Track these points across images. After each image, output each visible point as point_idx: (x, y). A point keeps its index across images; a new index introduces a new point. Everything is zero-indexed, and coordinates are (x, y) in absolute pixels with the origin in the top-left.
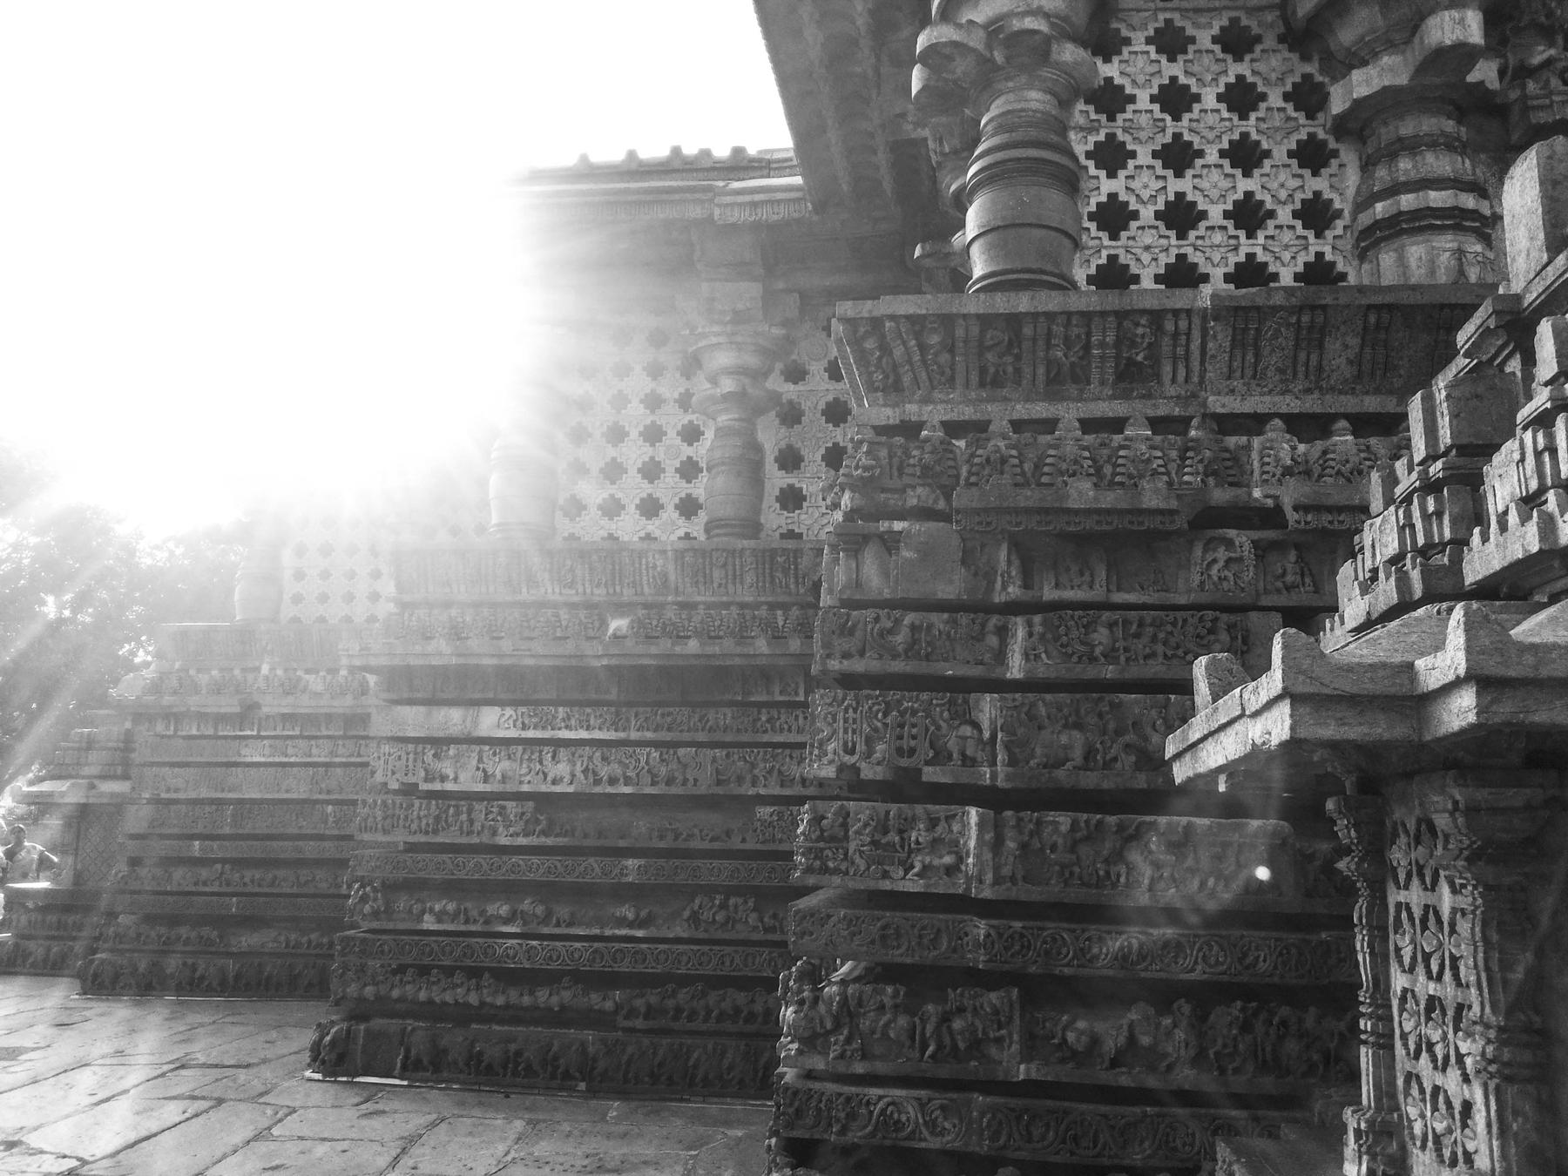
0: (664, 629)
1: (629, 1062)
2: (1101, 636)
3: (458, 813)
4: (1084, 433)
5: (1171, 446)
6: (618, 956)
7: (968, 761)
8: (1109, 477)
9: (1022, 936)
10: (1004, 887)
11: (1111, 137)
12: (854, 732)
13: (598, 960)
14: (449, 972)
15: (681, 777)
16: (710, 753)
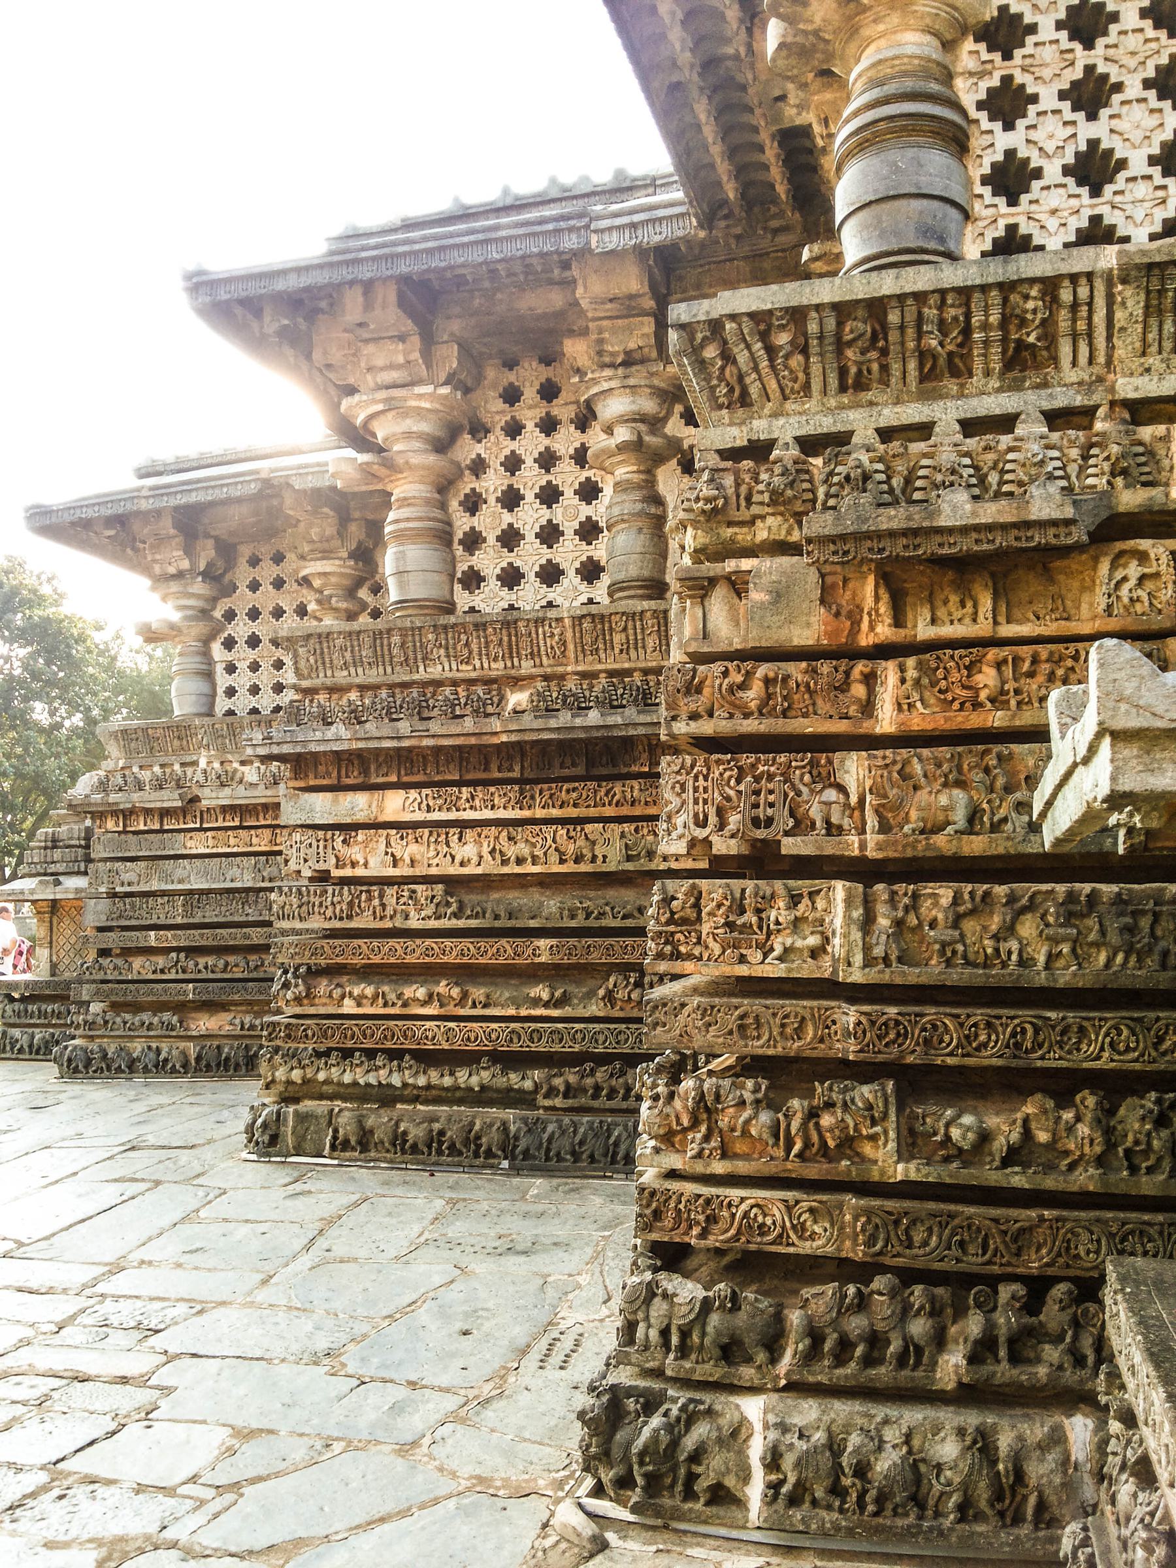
0: (564, 702)
1: (550, 1140)
2: (987, 678)
3: (370, 899)
4: (965, 437)
5: (1072, 443)
6: (535, 1036)
7: (832, 829)
8: (995, 487)
9: (897, 1023)
10: (876, 969)
11: (1007, 80)
12: (705, 802)
14: (371, 1054)
15: (589, 855)
16: (616, 828)
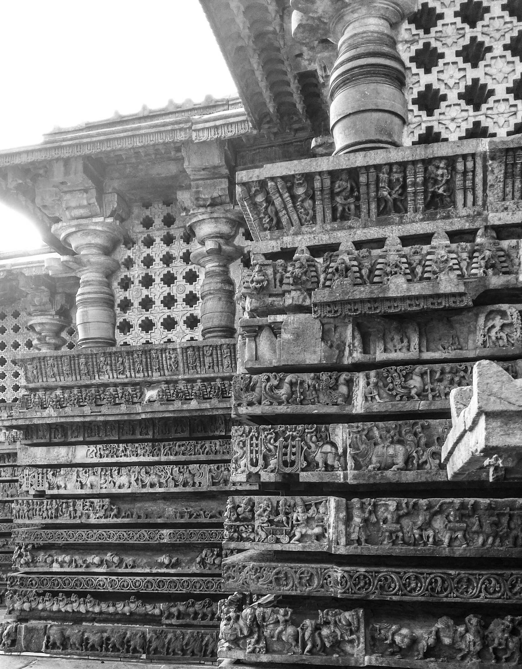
0: (177, 395)
1: (169, 643)
2: (416, 382)
3: (67, 507)
6: (161, 584)
7: (328, 468)
9: (365, 577)
10: (353, 546)
13: (150, 586)
15: (191, 482)
16: (207, 467)
